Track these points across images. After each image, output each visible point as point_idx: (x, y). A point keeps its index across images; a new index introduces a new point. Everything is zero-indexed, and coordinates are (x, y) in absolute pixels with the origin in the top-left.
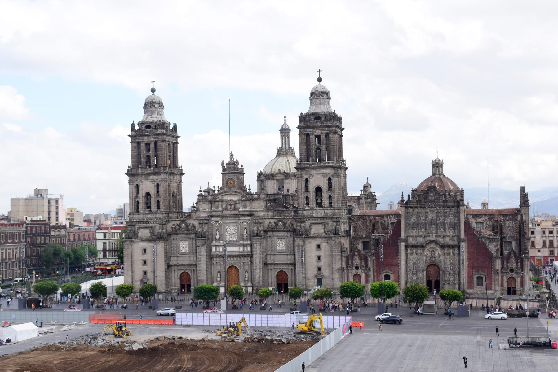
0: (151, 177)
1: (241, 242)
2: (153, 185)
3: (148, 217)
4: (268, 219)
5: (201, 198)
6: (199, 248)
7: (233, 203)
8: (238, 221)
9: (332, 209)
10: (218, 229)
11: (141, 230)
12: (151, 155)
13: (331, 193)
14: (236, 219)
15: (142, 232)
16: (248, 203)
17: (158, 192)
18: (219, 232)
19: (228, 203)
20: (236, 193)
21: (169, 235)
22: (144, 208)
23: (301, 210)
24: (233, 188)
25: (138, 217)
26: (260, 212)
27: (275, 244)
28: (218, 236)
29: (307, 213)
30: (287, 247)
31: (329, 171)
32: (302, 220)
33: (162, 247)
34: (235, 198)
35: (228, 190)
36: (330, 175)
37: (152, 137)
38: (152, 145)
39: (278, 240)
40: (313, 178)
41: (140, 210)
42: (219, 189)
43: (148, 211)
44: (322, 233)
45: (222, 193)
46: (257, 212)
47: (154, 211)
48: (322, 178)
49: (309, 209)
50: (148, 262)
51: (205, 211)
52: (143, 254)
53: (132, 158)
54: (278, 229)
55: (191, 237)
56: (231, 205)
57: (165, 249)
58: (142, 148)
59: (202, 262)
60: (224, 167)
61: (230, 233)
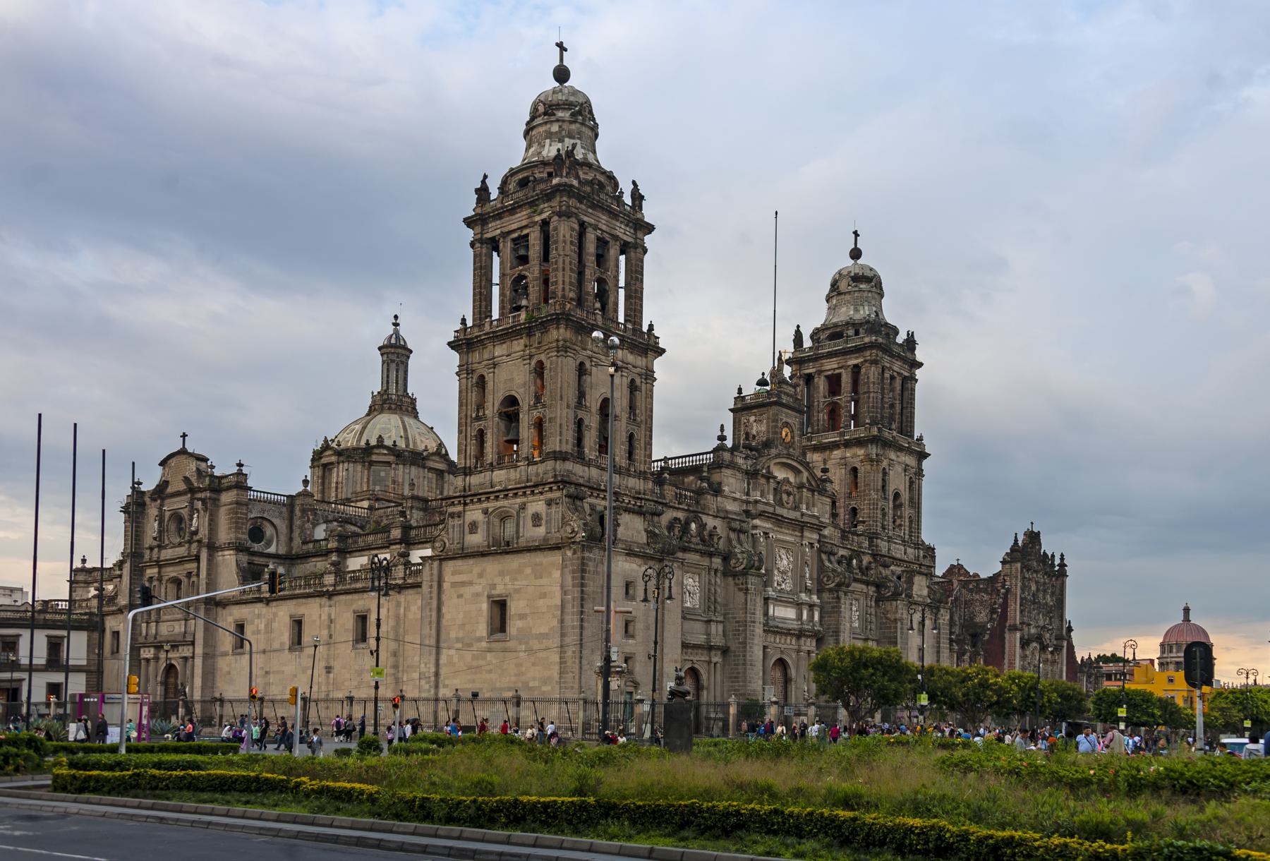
1: (803, 596)
2: (624, 378)
7: (791, 489)
8: (798, 540)
17: (632, 407)
19: (784, 488)
20: (798, 466)
24: (791, 450)
25: (581, 474)
31: (910, 461)
34: (792, 480)
35: (785, 452)
41: (586, 450)
50: (639, 627)
55: (714, 566)
59: (756, 641)
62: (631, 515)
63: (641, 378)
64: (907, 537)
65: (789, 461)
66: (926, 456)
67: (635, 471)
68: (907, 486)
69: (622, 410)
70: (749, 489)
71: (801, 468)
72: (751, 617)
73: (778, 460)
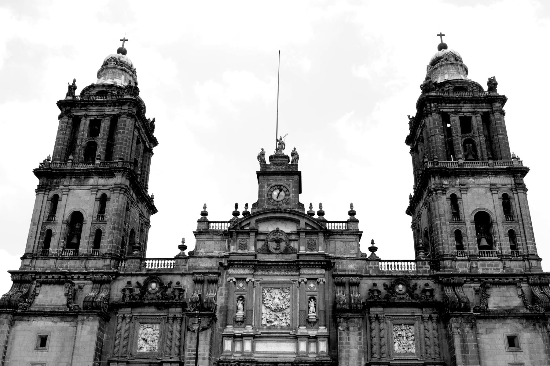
0: (92, 181)
1: (303, 330)
2: (94, 196)
3: (66, 267)
4: (370, 276)
5: (204, 226)
6: (191, 339)
7: (283, 237)
8: (295, 278)
9: (519, 260)
10: (241, 298)
11: (45, 288)
12: (99, 143)
13: (513, 226)
14: (290, 273)
15: (47, 292)
16: (321, 237)
17: (102, 211)
18: (243, 304)
19: (272, 237)
20: (292, 216)
21: (115, 307)
22: (62, 244)
23: (447, 259)
24: (284, 205)
25: (42, 266)
26: (348, 261)
27: (388, 337)
28: (240, 313)
29: (461, 267)
30: (421, 345)
32: (456, 280)
33: (91, 332)
36: (506, 188)
37: (108, 108)
38: (105, 124)
39: (396, 327)
40: (469, 194)
41: (51, 249)
42: (250, 210)
43: (70, 253)
44: (516, 308)
45: (259, 214)
46: (340, 261)
47: (85, 252)
48: (489, 194)
49: (466, 258)
51: (211, 254)
52: (37, 348)
53: (57, 144)
54: (397, 301)
55: (171, 315)
56: (278, 241)
57: (99, 340)
58: (82, 128)
60: (265, 162)
61: (273, 307)
62: (51, 286)
63: (111, 191)
64: (507, 250)
65: (278, 215)
66: (524, 171)
67: (98, 255)
68: (499, 203)
69: (89, 216)
70: (229, 247)
71: (296, 217)
72: (189, 354)
73: (261, 217)
